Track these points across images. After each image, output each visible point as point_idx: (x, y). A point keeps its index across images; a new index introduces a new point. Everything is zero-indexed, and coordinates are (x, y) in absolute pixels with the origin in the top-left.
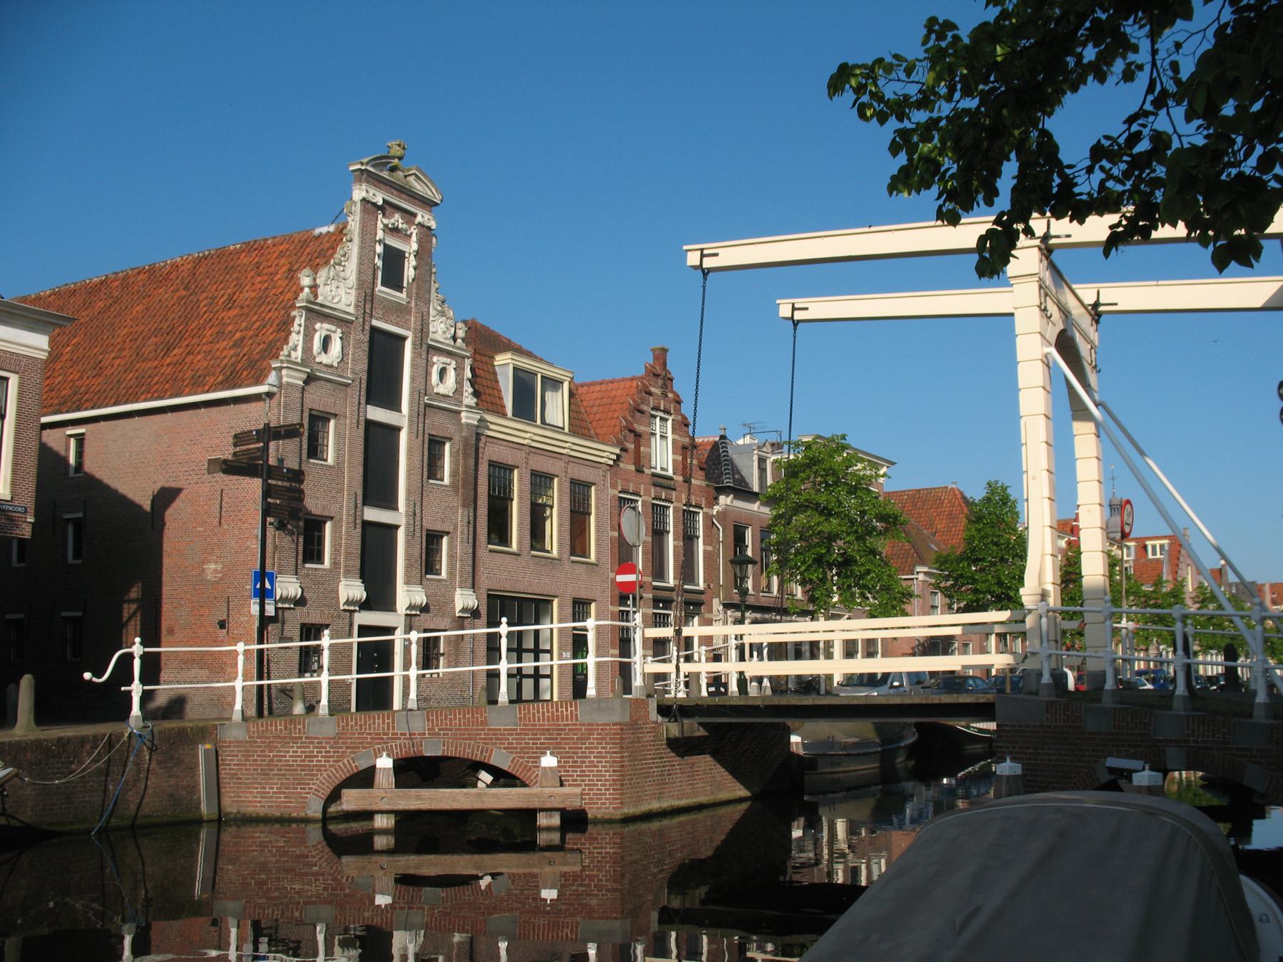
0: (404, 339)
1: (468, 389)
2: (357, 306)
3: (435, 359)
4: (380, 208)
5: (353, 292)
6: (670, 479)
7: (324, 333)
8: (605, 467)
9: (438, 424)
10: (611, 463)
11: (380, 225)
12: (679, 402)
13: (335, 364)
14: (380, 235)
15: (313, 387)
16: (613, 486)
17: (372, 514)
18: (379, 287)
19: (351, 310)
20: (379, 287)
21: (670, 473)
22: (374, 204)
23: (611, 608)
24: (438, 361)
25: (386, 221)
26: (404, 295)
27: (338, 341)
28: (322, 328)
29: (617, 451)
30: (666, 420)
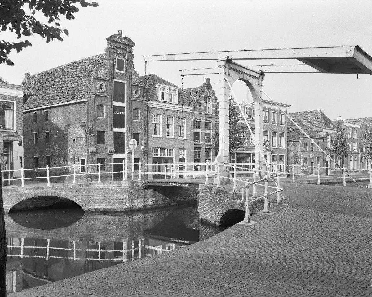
0: (125, 83)
6: (211, 115)
7: (100, 84)
8: (189, 113)
9: (135, 105)
10: (191, 112)
11: (115, 53)
12: (214, 93)
13: (104, 92)
14: (115, 56)
15: (97, 99)
16: (193, 118)
17: (116, 130)
18: (116, 71)
20: (116, 71)
21: (211, 113)
22: (113, 49)
23: (192, 151)
27: (105, 86)
28: (99, 83)
29: (193, 108)
30: (210, 98)
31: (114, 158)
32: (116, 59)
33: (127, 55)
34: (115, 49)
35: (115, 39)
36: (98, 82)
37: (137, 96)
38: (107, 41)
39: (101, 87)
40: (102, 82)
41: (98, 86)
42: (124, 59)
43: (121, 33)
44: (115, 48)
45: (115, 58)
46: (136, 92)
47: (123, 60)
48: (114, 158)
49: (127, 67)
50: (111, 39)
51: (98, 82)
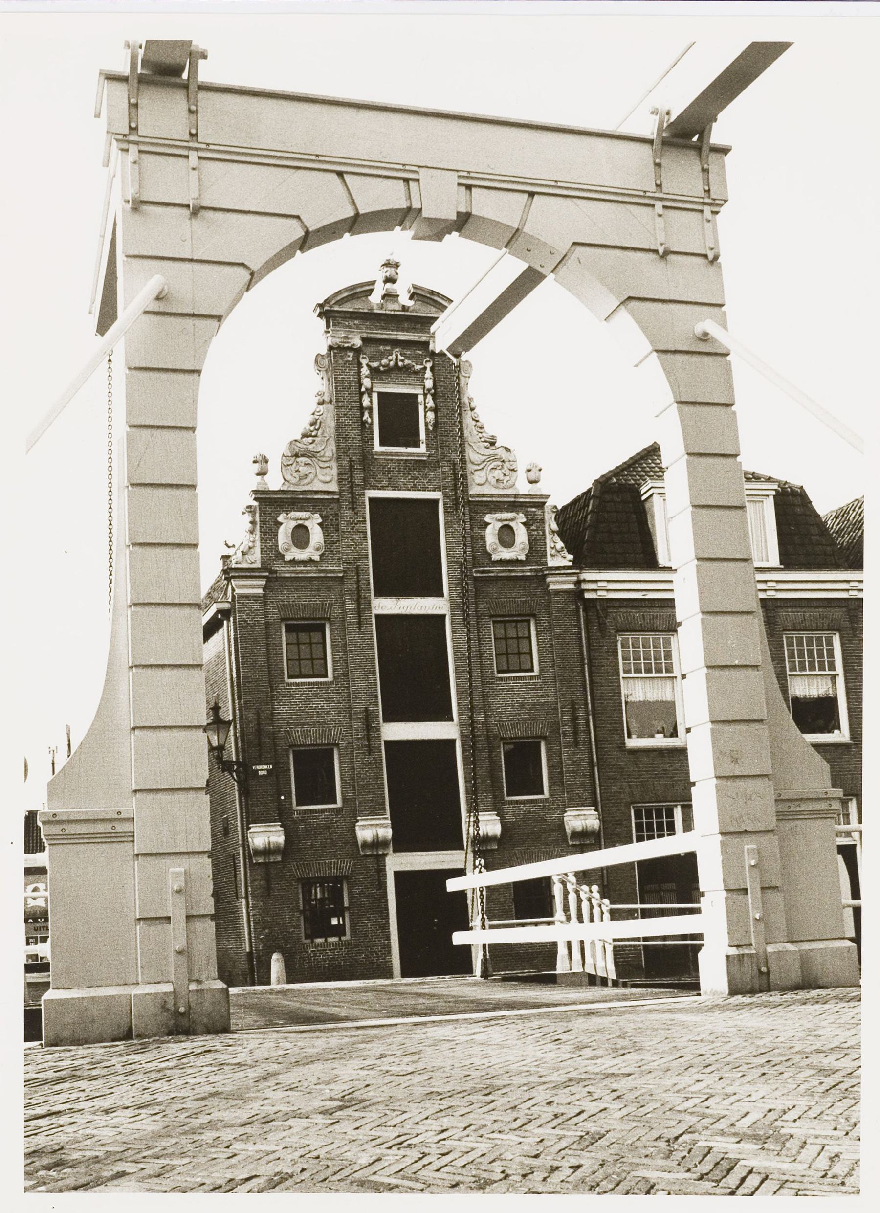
1: (554, 543)
2: (340, 481)
3: (488, 518)
4: (358, 351)
5: (334, 464)
7: (294, 524)
11: (365, 371)
13: (317, 558)
14: (367, 382)
18: (378, 448)
19: (334, 487)
24: (494, 521)
25: (375, 364)
26: (422, 449)
31: (397, 874)
32: (375, 397)
36: (280, 519)
37: (506, 554)
39: (300, 536)
42: (418, 391)
44: (358, 342)
45: (370, 392)
46: (506, 535)
47: (416, 396)
48: (397, 874)
49: (436, 425)
50: (329, 313)
51: (280, 519)
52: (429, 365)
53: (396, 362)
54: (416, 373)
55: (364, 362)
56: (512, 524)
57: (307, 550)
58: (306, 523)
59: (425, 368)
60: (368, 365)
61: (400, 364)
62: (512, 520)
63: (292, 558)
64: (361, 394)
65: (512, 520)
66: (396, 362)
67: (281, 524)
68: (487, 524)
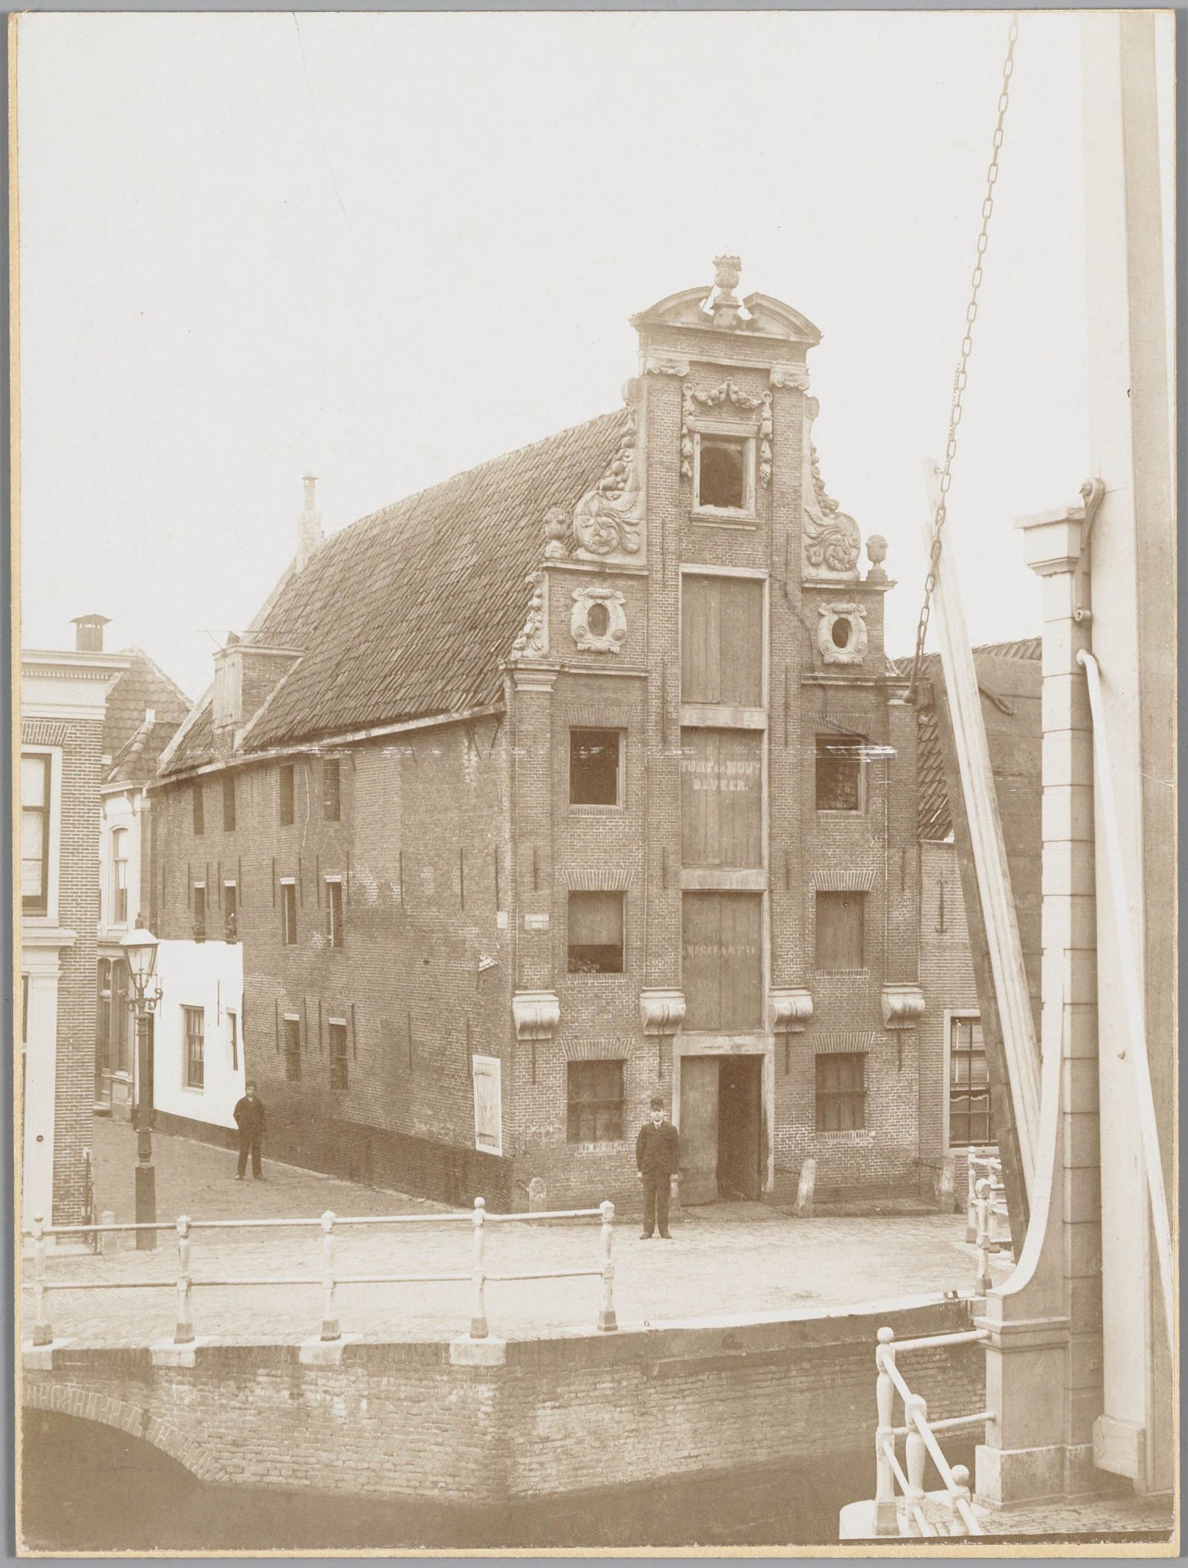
7: (591, 603)
33: (767, 408)
34: (682, 379)
35: (688, 319)
38: (634, 336)
39: (599, 618)
40: (599, 589)
41: (579, 616)
43: (730, 267)
51: (575, 595)
52: (768, 401)
53: (728, 395)
54: (751, 410)
55: (688, 393)
56: (850, 618)
57: (604, 638)
58: (607, 603)
59: (763, 404)
60: (694, 397)
61: (734, 397)
62: (849, 613)
63: (587, 646)
64: (683, 436)
65: (849, 613)
66: (728, 395)
67: (575, 601)
68: (821, 616)
